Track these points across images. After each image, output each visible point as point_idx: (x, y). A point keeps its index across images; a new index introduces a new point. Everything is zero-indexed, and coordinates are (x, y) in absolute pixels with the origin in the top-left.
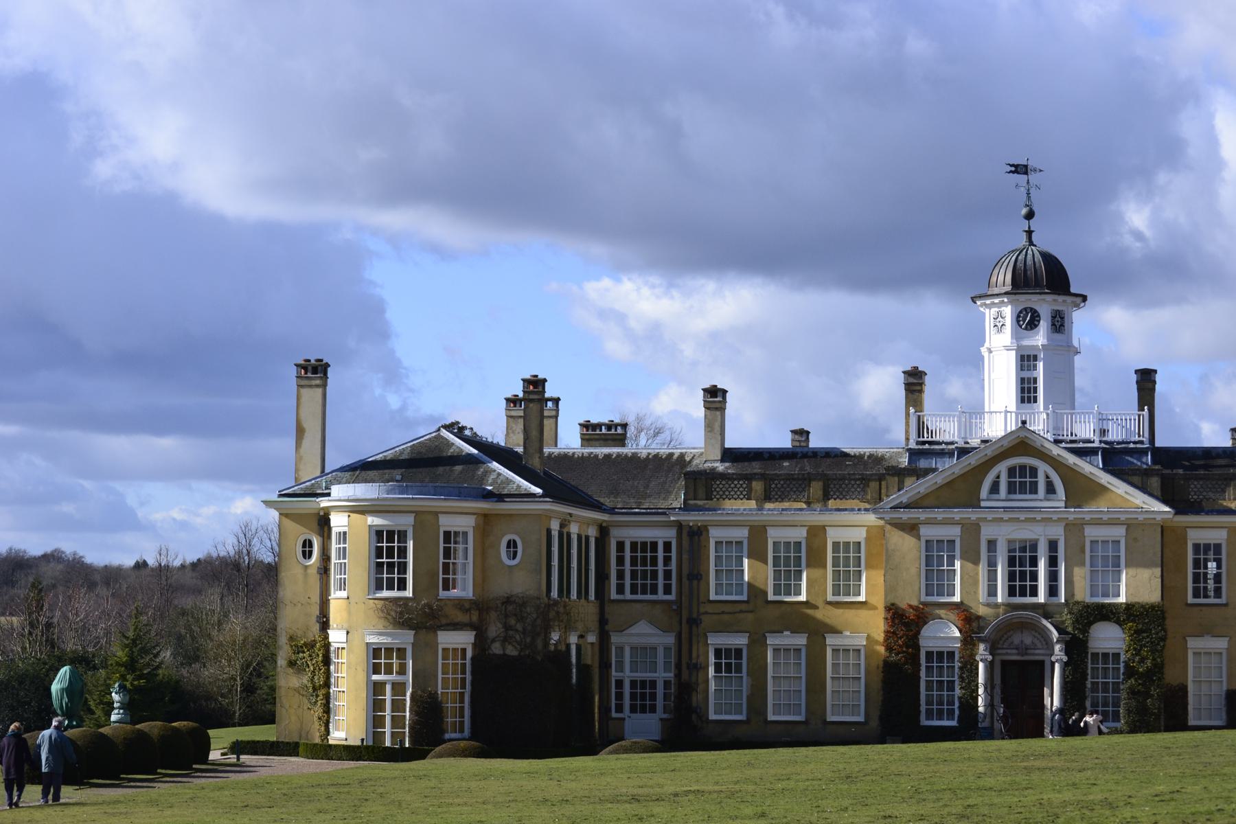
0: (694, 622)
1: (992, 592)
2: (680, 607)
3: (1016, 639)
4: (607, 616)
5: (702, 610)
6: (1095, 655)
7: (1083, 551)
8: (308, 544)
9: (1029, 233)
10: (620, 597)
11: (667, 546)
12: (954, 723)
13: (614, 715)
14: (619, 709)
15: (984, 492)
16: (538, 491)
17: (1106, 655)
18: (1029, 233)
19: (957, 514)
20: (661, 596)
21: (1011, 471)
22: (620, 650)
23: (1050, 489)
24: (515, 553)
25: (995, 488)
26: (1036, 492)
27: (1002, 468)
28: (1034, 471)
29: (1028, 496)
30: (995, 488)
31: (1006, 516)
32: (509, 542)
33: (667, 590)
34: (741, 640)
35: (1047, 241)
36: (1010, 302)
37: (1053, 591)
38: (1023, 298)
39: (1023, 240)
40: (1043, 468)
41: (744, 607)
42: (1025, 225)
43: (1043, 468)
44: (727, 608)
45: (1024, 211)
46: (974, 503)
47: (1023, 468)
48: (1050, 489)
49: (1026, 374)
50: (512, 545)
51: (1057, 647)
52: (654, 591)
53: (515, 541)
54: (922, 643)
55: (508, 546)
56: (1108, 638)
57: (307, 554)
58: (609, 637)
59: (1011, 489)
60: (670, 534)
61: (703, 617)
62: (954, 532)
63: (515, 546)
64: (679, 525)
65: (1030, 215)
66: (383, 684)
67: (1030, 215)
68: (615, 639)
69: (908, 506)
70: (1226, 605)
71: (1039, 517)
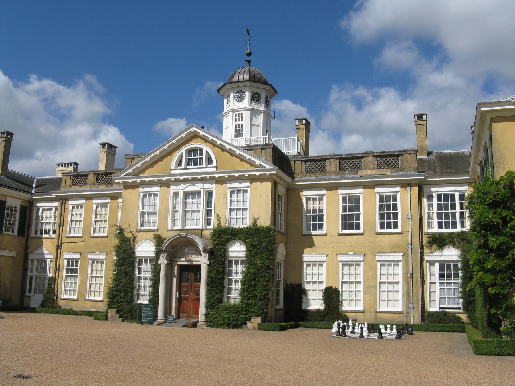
4: (29, 245)
5: (63, 242)
7: (225, 197)
13: (27, 294)
14: (30, 292)
21: (189, 152)
22: (33, 261)
26: (201, 163)
27: (183, 150)
30: (180, 163)
34: (77, 256)
41: (80, 239)
43: (206, 148)
47: (196, 150)
48: (209, 160)
56: (237, 250)
58: (28, 255)
59: (189, 162)
68: (31, 256)
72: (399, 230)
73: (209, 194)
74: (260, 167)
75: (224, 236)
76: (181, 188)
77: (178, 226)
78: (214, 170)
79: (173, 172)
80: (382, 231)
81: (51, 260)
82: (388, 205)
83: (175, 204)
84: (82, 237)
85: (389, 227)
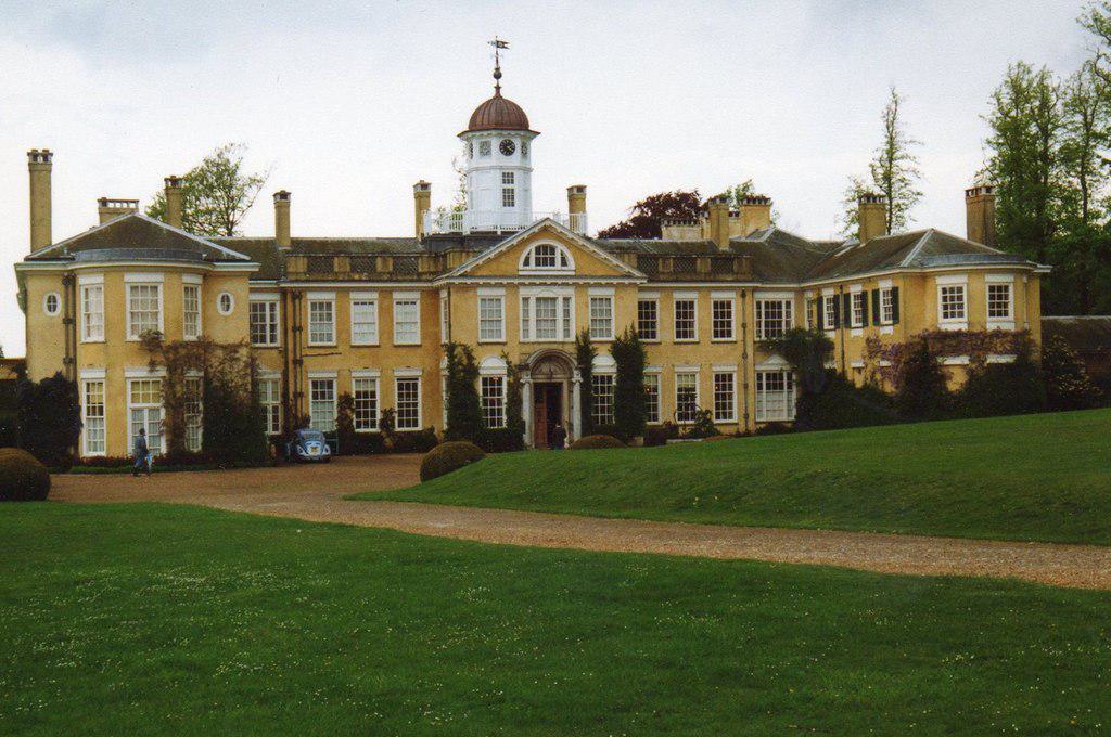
0: (298, 362)
1: (526, 331)
2: (286, 349)
3: (545, 368)
6: (596, 378)
8: (52, 300)
9: (498, 88)
10: (273, 345)
11: (272, 306)
16: (247, 258)
17: (603, 377)
18: (498, 88)
20: (269, 344)
21: (538, 250)
23: (564, 262)
24: (228, 306)
25: (527, 263)
26: (553, 264)
27: (532, 247)
28: (553, 250)
29: (549, 267)
30: (527, 263)
31: (538, 281)
32: (223, 297)
33: (273, 340)
37: (567, 332)
38: (505, 133)
40: (560, 247)
42: (494, 82)
43: (560, 247)
44: (322, 352)
48: (564, 262)
51: (575, 372)
52: (263, 340)
54: (481, 371)
55: (223, 301)
57: (52, 308)
59: (538, 264)
60: (276, 297)
61: (304, 359)
63: (228, 300)
64: (284, 292)
65: (498, 76)
66: (140, 410)
67: (498, 76)
70: (698, 343)
71: (549, 282)
73: (566, 300)
74: (629, 276)
76: (534, 293)
78: (573, 273)
79: (520, 273)
80: (716, 340)
81: (275, 382)
82: (722, 310)
83: (526, 312)
84: (336, 347)
85: (723, 336)
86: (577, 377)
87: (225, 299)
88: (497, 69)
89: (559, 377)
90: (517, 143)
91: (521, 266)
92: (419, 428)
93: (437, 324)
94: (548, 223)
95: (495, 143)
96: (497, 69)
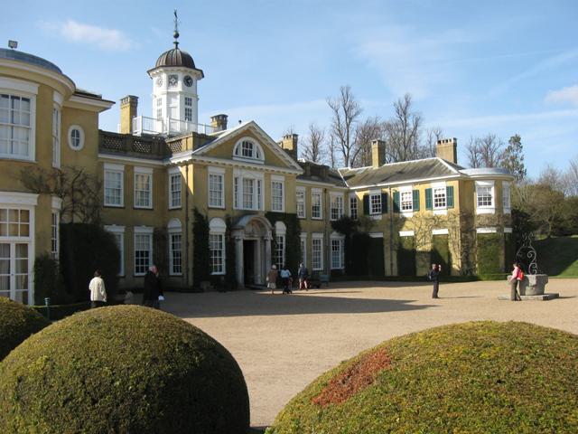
9: (177, 43)
12: (223, 272)
15: (234, 154)
18: (177, 43)
19: (228, 162)
24: (78, 141)
27: (241, 141)
32: (73, 132)
35: (183, 48)
36: (165, 71)
39: (174, 46)
40: (256, 144)
42: (175, 40)
45: (174, 33)
46: (230, 158)
47: (247, 143)
49: (188, 107)
50: (75, 133)
53: (77, 131)
55: (73, 135)
56: (281, 228)
62: (221, 171)
63: (78, 135)
65: (177, 36)
67: (177, 36)
69: (203, 155)
72: (321, 218)
74: (294, 168)
75: (273, 217)
77: (241, 207)
86: (269, 237)
87: (75, 133)
88: (176, 31)
89: (257, 237)
90: (194, 78)
91: (234, 154)
92: (172, 273)
93: (165, 194)
94: (251, 125)
95: (181, 76)
96: (176, 31)
